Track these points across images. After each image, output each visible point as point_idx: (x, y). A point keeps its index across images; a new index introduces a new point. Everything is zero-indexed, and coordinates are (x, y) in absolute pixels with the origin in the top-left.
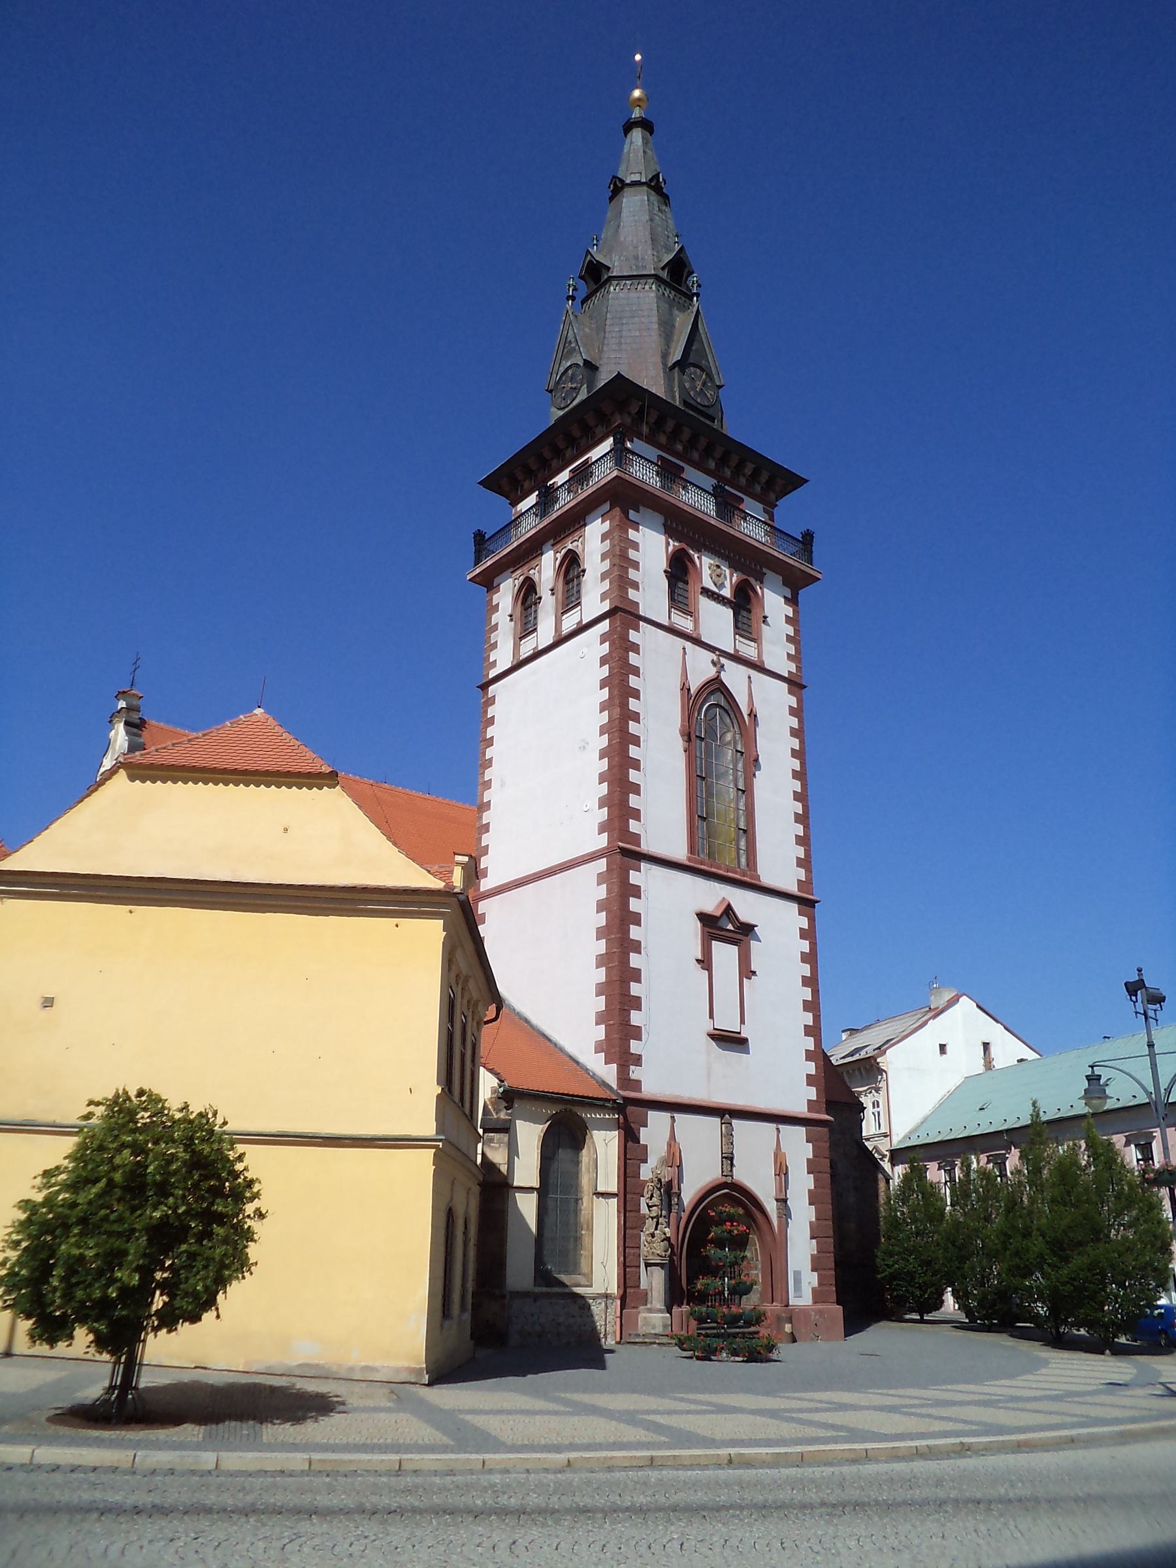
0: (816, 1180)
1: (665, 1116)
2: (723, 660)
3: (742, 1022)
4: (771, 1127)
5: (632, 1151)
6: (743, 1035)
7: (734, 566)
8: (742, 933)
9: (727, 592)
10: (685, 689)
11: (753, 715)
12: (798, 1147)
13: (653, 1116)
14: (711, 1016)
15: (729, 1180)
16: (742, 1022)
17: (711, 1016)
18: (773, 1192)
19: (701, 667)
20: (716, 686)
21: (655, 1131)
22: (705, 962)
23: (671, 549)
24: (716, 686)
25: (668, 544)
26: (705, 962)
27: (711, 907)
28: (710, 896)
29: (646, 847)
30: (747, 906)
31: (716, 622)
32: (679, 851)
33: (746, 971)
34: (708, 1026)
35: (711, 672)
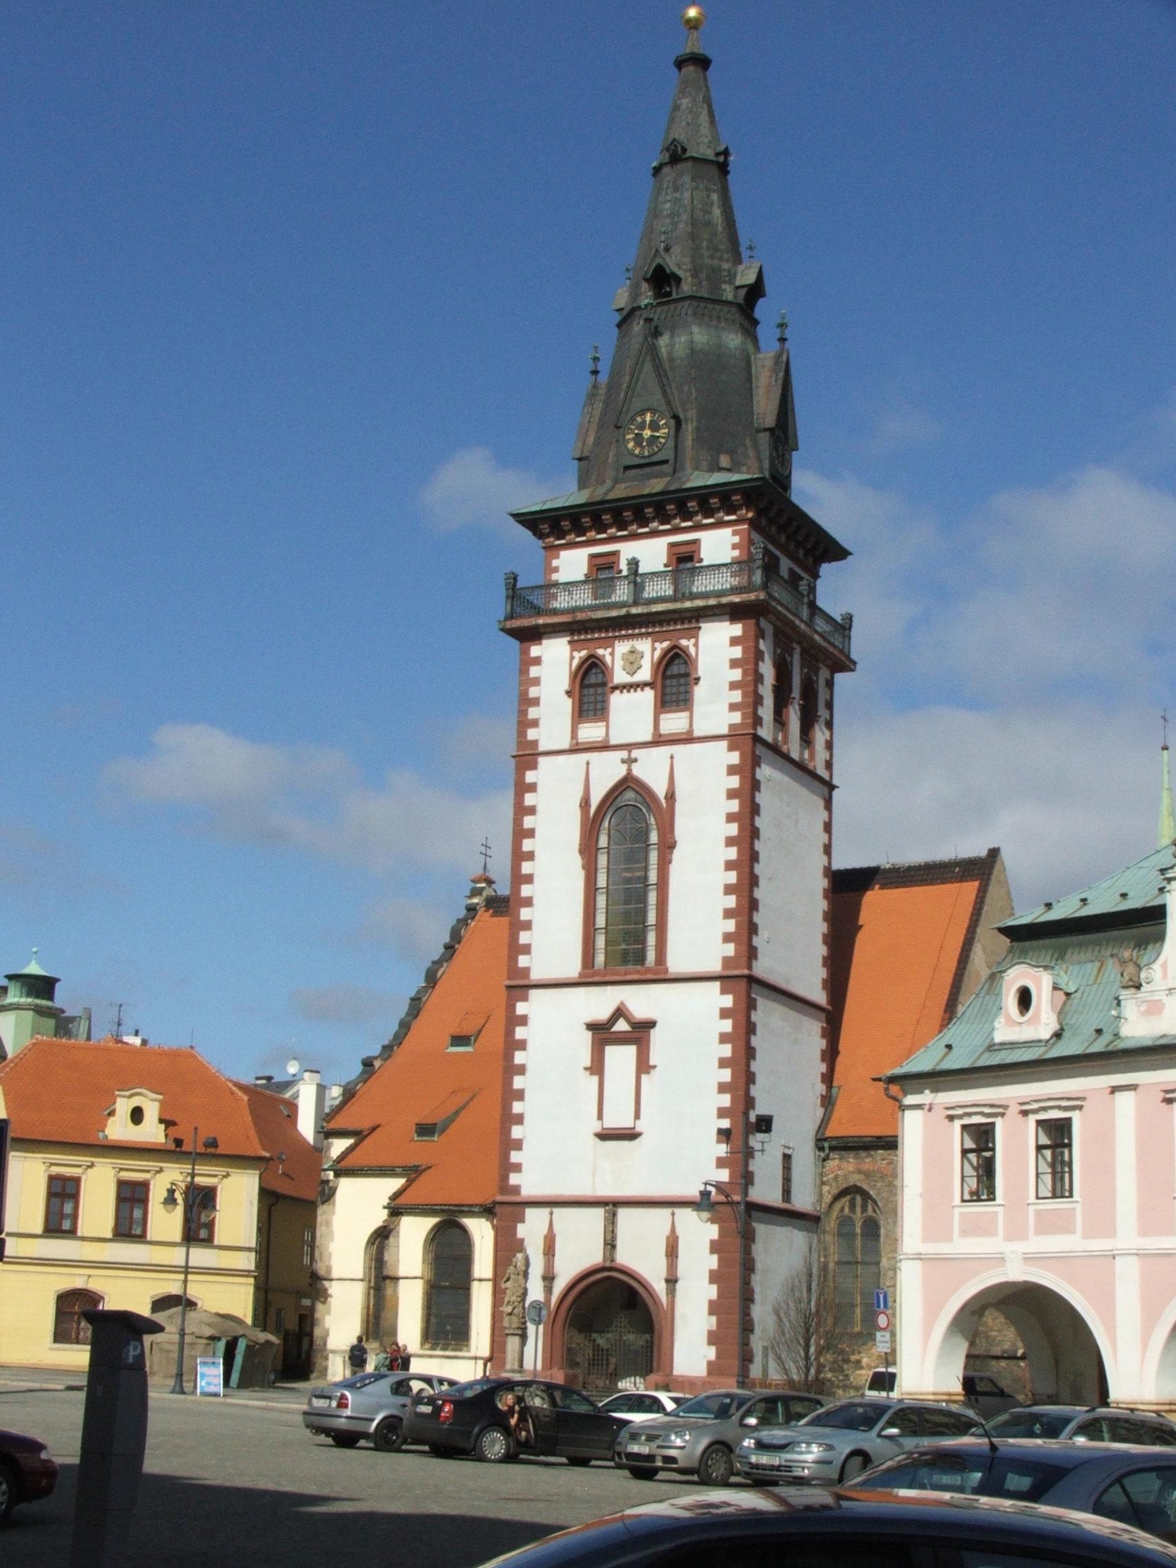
0: (720, 1259)
1: (544, 1212)
2: (635, 753)
3: (637, 1116)
4: (665, 1213)
5: (507, 1247)
6: (638, 1129)
7: (657, 637)
8: (641, 1032)
9: (645, 674)
10: (585, 803)
11: (671, 796)
12: (698, 1233)
13: (530, 1212)
14: (600, 1117)
15: (608, 1264)
16: (637, 1116)
17: (600, 1117)
18: (664, 1275)
19: (607, 772)
20: (628, 783)
21: (532, 1228)
22: (597, 1067)
23: (576, 662)
24: (628, 783)
25: (572, 658)
26: (597, 1067)
27: (603, 1014)
28: (600, 1003)
29: (535, 976)
30: (641, 1001)
31: (632, 713)
32: (572, 967)
33: (644, 1066)
34: (597, 1127)
35: (621, 771)
